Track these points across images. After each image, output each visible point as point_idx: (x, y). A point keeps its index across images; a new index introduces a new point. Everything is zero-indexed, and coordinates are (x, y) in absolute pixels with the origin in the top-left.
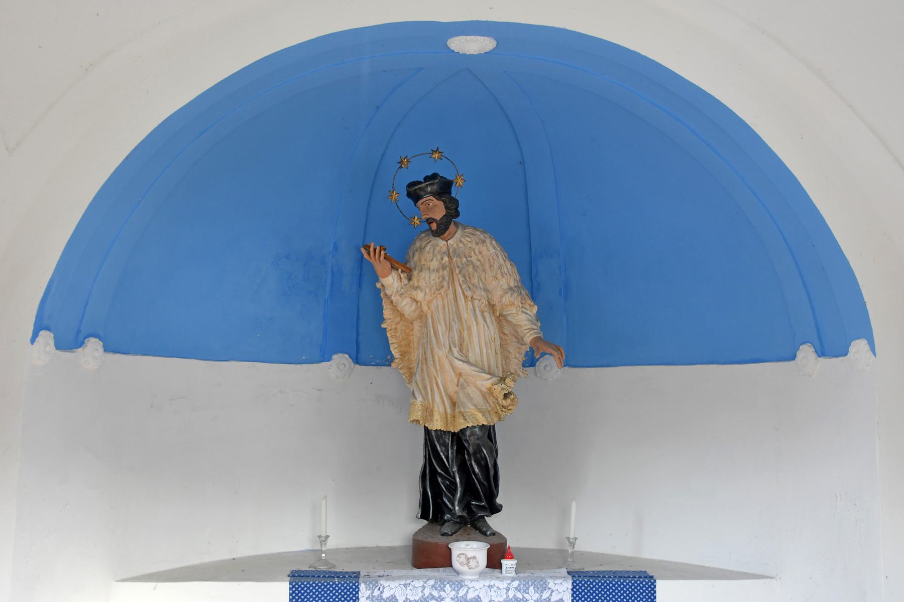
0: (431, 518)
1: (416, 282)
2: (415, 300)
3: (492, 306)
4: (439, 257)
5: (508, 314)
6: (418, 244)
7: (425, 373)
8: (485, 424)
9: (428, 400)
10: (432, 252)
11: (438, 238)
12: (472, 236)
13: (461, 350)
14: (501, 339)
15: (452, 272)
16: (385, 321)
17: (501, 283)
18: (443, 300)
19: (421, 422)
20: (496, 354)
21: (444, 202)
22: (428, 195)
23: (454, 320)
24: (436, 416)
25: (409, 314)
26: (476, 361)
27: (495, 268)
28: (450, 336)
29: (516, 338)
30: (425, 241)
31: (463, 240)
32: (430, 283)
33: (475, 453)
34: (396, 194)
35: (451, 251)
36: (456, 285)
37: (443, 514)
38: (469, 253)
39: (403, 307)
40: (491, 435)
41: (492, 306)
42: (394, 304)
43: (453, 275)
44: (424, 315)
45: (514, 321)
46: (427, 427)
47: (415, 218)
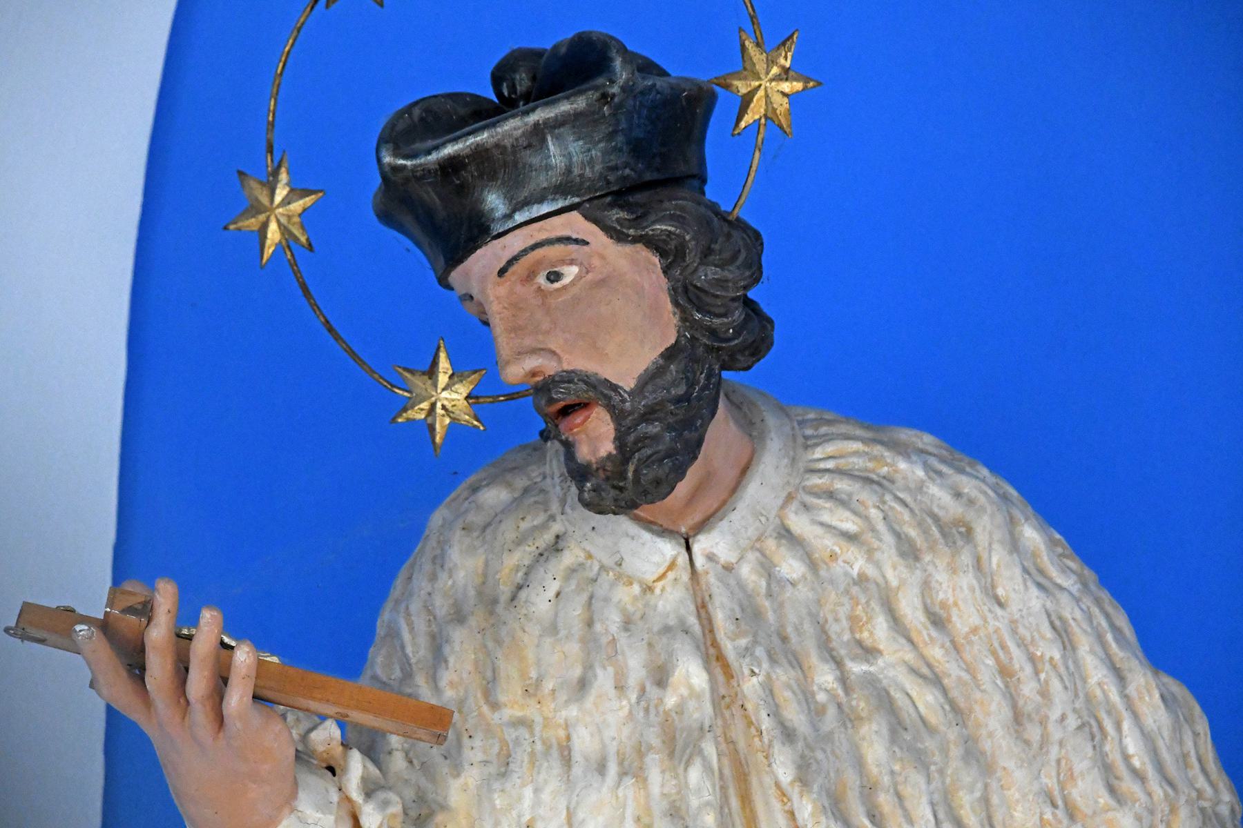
4: (636, 664)
10: (578, 628)
11: (623, 523)
12: (866, 496)
22: (545, 208)
27: (1056, 733)
31: (799, 523)
35: (720, 618)
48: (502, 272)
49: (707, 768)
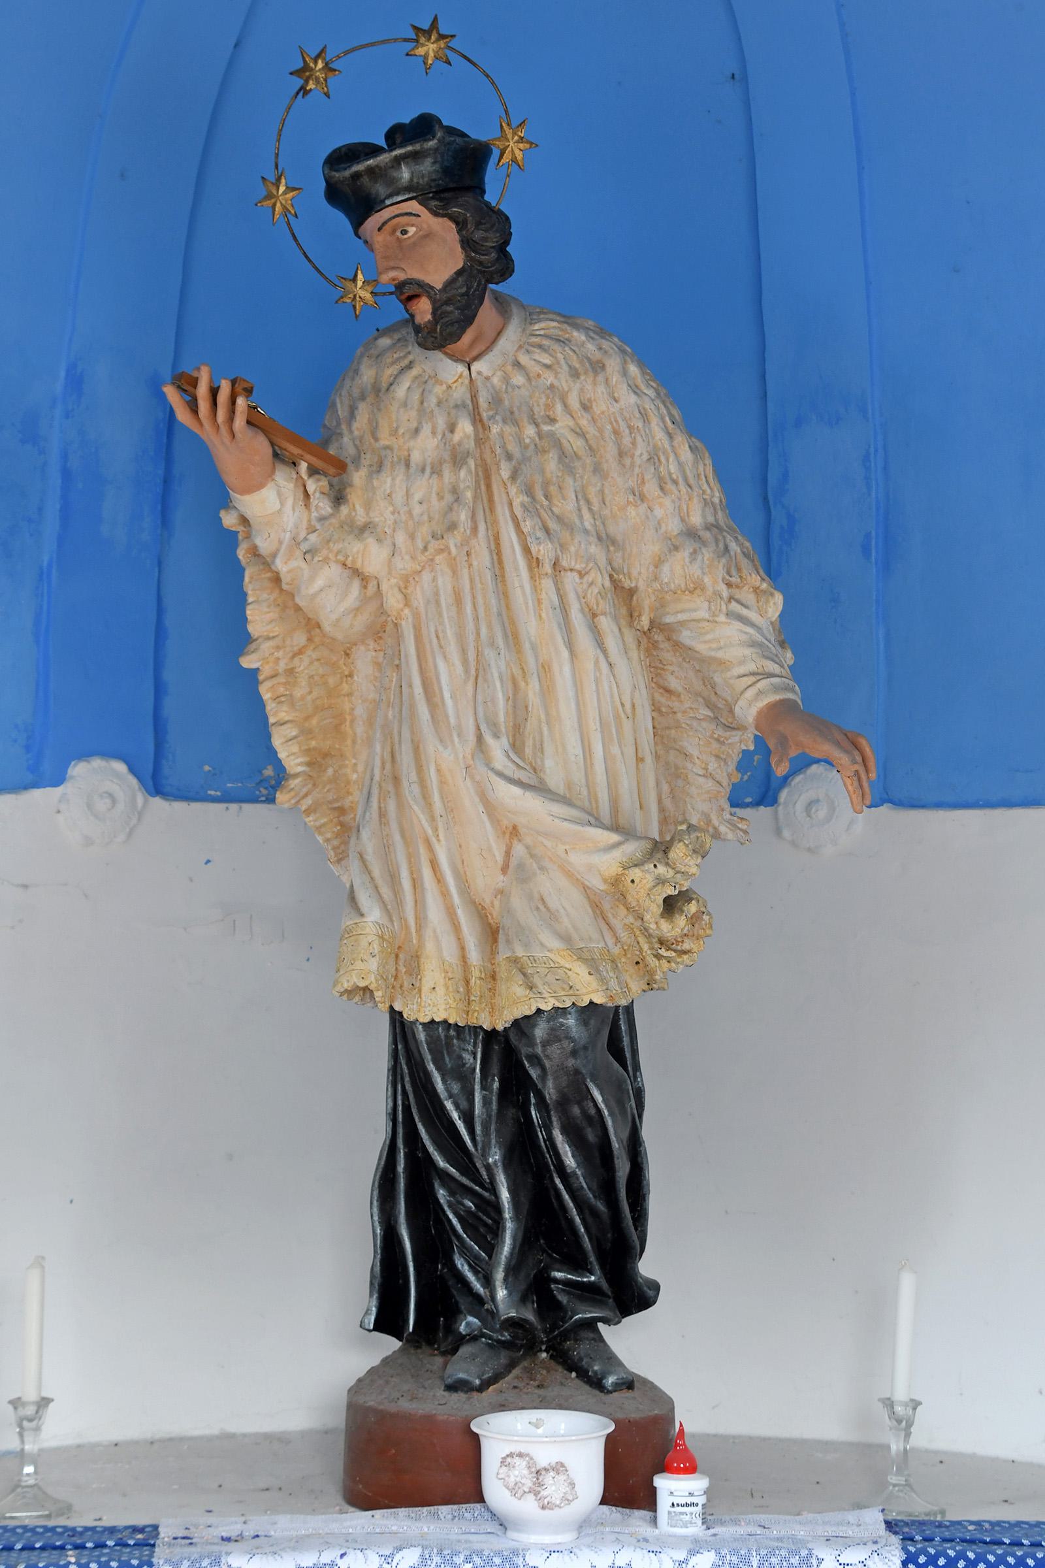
0: (411, 1330)
1: (360, 511)
2: (356, 573)
3: (625, 595)
4: (441, 422)
5: (682, 623)
6: (367, 374)
7: (394, 825)
8: (598, 999)
9: (403, 920)
10: (416, 404)
11: (438, 355)
12: (556, 347)
13: (516, 747)
14: (656, 708)
15: (486, 475)
16: (253, 646)
17: (659, 512)
18: (454, 572)
19: (378, 995)
20: (640, 760)
21: (457, 223)
23: (492, 644)
24: (432, 975)
25: (338, 620)
26: (569, 785)
27: (638, 461)
28: (480, 698)
29: (709, 705)
30: (393, 363)
31: (524, 359)
32: (410, 513)
33: (563, 1103)
34: (289, 189)
36: (501, 518)
37: (453, 1313)
38: (548, 407)
39: (314, 596)
40: (620, 1040)
41: (625, 595)
42: (285, 587)
43: (489, 486)
44: (390, 627)
45: (701, 648)
46: (400, 1014)
47: (354, 280)
48: (379, 229)
49: (470, 471)
